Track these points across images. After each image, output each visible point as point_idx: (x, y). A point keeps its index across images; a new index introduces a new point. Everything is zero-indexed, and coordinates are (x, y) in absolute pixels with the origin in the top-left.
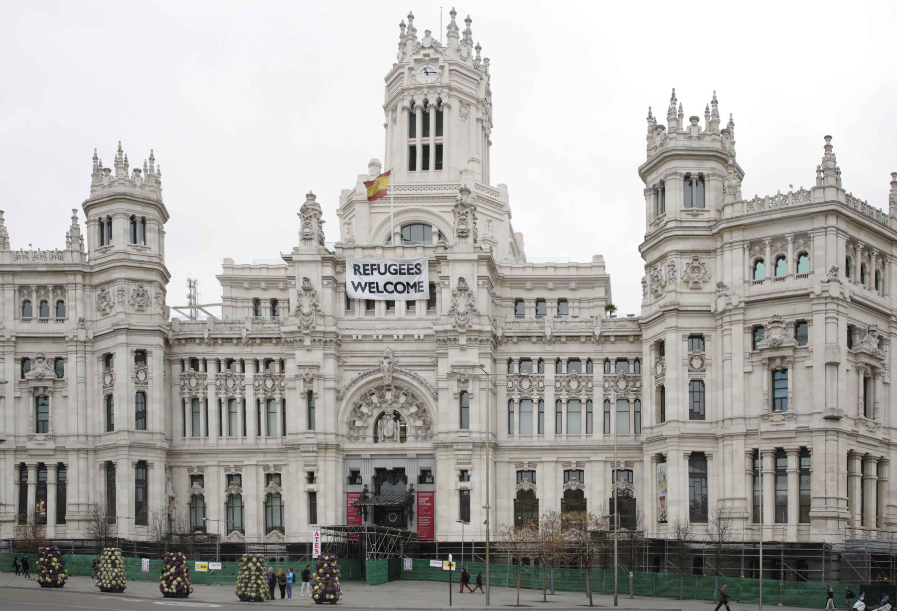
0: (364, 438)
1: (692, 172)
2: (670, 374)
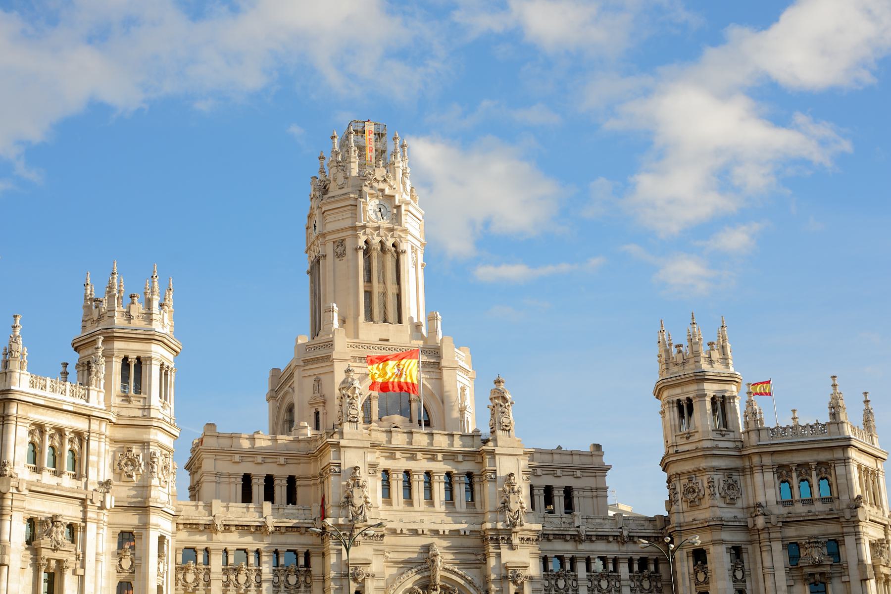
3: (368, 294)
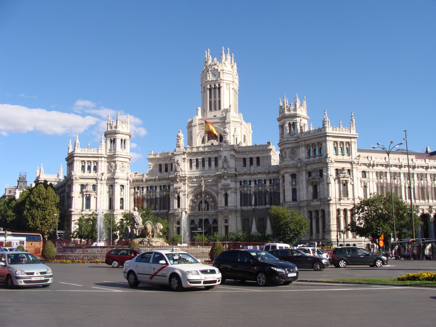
0: (195, 210)
1: (291, 122)
2: (286, 187)
3: (210, 102)
